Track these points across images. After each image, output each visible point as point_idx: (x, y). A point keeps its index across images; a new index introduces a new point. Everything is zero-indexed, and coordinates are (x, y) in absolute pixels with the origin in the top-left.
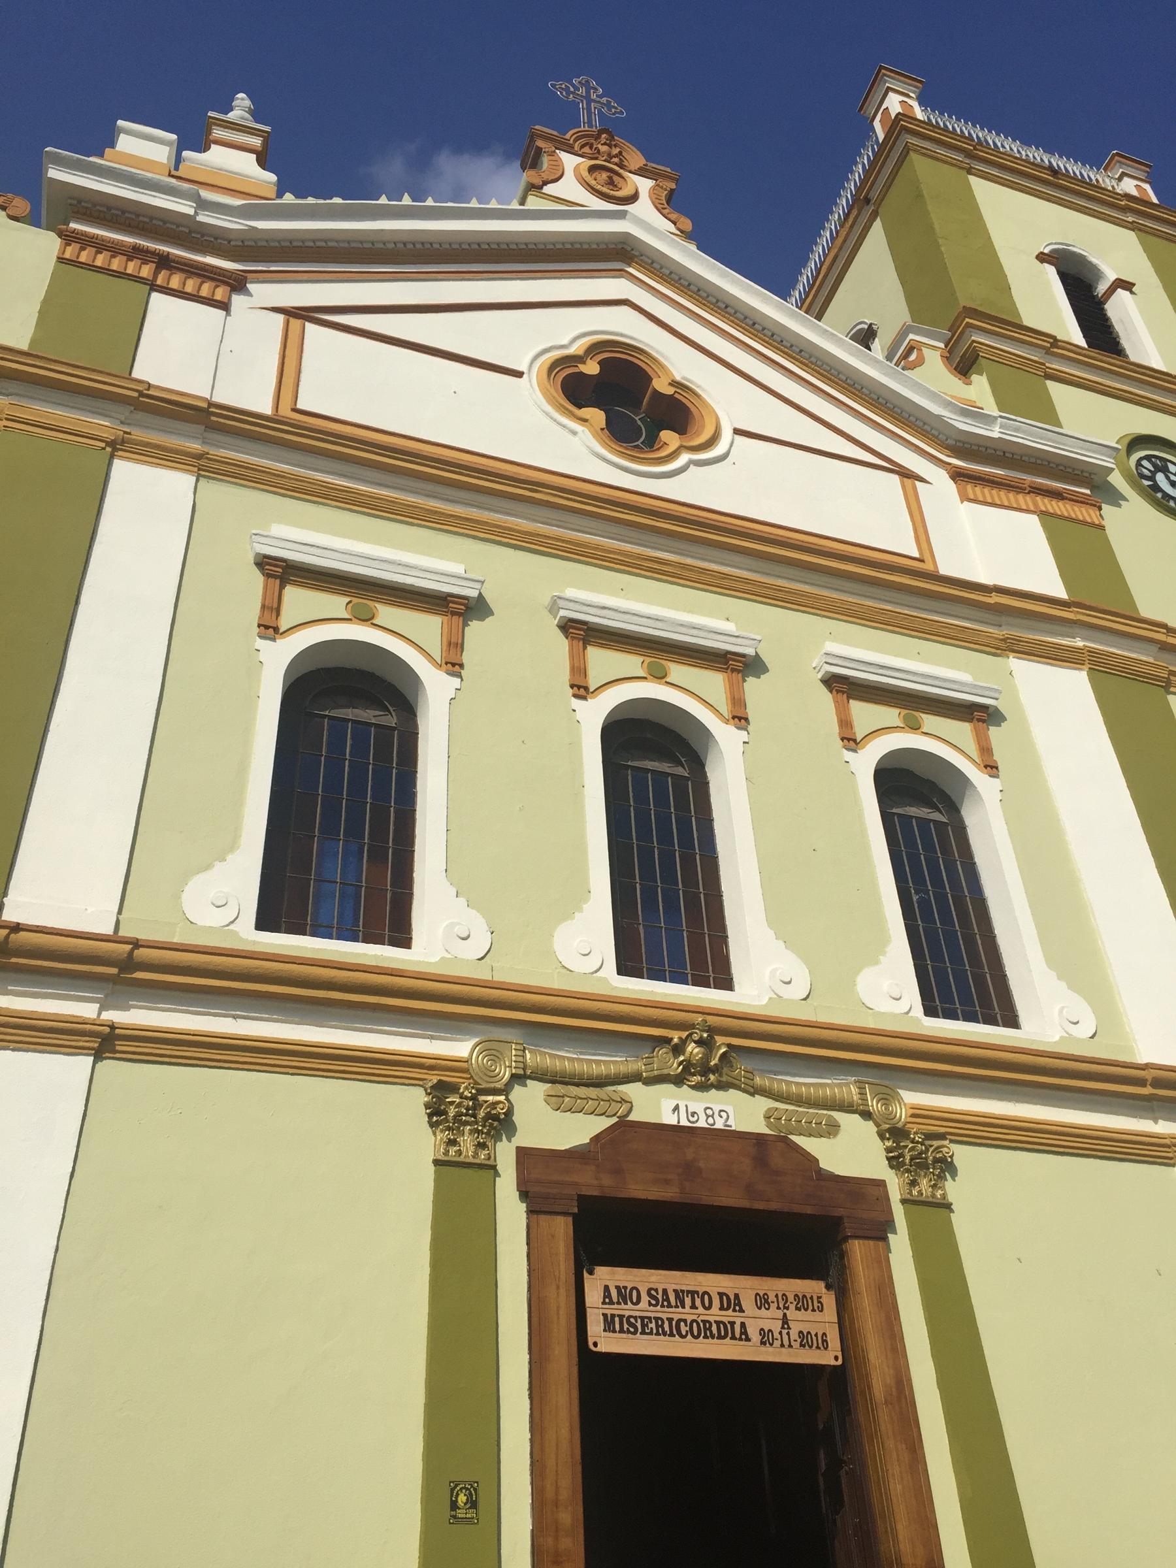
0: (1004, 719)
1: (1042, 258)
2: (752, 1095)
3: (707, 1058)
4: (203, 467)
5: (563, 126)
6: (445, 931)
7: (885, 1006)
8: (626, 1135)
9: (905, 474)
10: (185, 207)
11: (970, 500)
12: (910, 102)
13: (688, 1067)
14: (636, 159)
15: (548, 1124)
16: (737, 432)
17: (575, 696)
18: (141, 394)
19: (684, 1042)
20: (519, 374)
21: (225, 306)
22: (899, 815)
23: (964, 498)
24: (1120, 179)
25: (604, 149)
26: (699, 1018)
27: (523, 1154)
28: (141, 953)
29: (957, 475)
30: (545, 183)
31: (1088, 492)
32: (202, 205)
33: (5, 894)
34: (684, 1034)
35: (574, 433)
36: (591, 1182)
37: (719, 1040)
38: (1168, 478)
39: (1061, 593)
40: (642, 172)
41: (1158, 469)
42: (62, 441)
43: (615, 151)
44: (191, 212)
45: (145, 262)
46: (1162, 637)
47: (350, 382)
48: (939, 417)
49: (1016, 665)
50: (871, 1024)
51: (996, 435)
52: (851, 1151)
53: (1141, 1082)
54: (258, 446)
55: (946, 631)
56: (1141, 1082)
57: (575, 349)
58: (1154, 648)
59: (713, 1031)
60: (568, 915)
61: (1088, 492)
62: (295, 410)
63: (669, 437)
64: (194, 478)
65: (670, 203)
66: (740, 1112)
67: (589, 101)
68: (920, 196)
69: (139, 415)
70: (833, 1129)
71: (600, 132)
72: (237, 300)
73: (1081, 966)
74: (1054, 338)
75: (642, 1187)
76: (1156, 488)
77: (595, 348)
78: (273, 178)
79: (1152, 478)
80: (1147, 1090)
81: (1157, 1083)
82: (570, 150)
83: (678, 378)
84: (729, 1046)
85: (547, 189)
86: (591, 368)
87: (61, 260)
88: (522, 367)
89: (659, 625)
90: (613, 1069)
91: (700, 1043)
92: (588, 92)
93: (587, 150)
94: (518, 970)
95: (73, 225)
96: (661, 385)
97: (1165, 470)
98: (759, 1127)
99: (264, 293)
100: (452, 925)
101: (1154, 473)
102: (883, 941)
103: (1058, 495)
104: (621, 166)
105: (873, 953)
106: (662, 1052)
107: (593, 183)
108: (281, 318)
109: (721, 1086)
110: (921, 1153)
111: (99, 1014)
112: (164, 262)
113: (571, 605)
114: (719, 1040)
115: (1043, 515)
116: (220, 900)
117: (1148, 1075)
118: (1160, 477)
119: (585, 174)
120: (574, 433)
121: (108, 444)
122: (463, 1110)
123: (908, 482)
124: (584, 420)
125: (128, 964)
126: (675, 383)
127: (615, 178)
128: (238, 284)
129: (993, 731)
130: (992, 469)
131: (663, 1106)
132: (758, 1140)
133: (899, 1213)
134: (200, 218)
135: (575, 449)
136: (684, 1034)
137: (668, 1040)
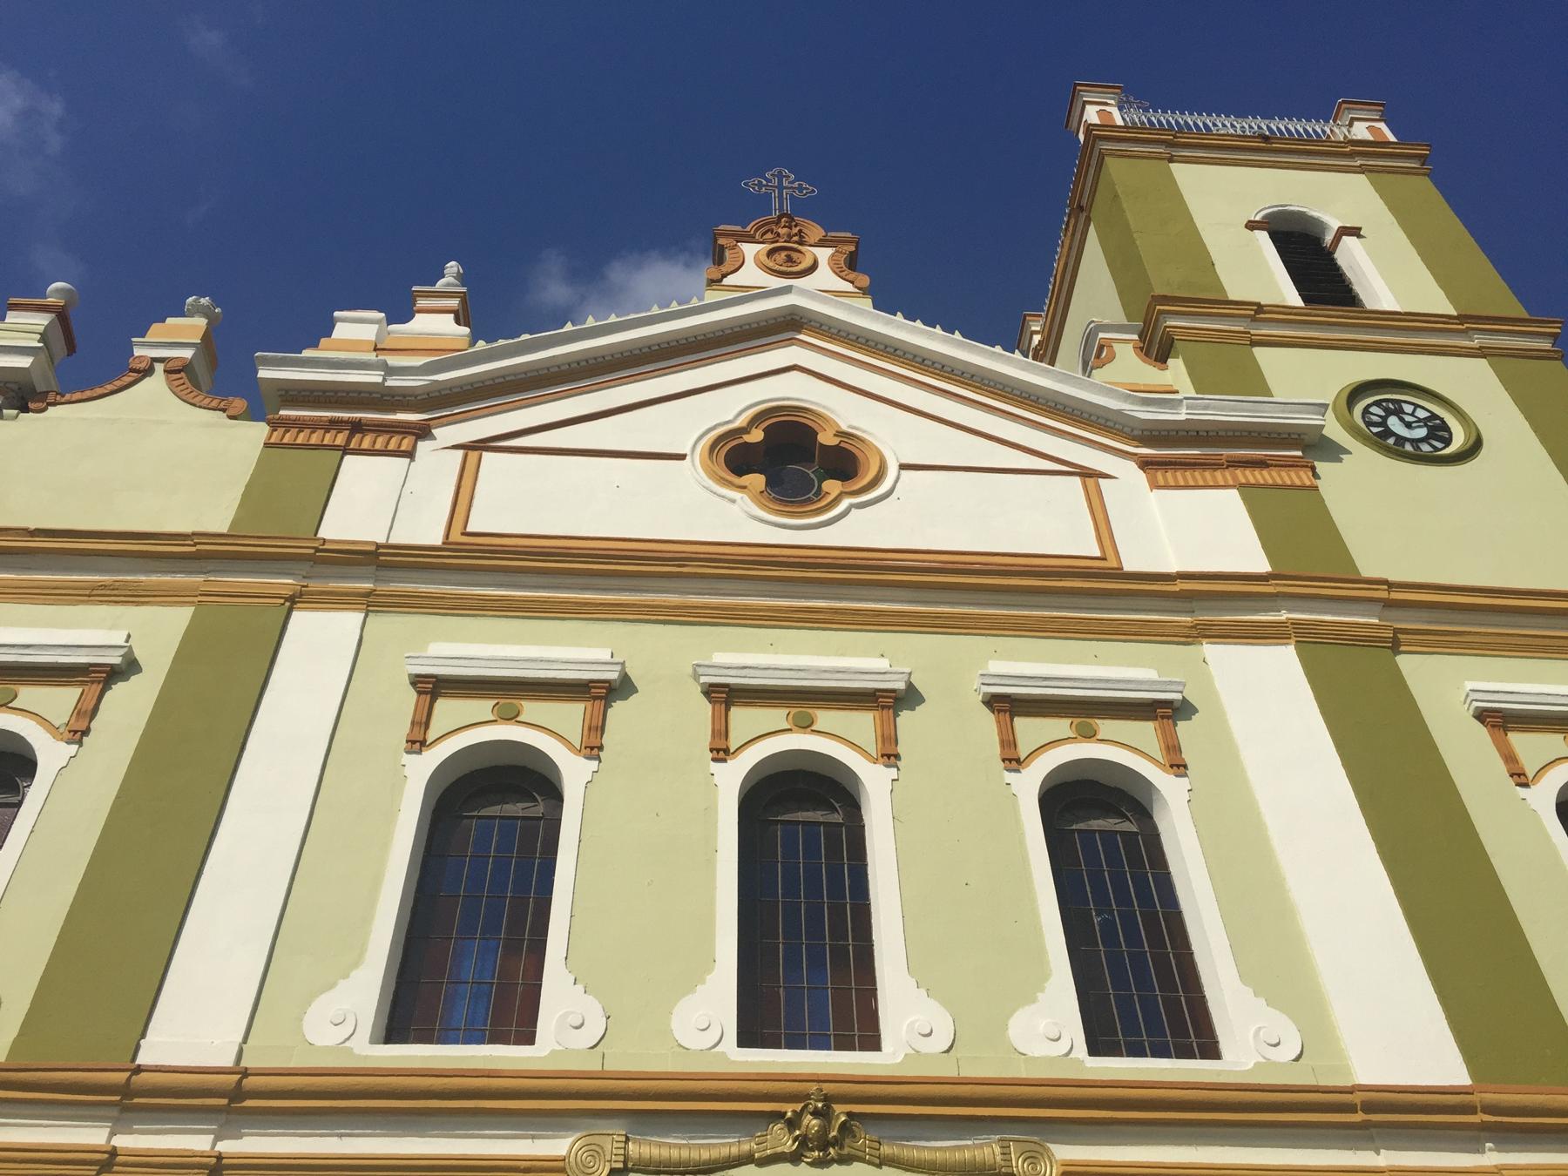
0: (1194, 710)
1: (1252, 226)
2: (879, 1166)
3: (824, 1130)
4: (371, 603)
5: (750, 215)
7: (1040, 1049)
9: (1087, 474)
10: (374, 377)
11: (1159, 487)
12: (1108, 108)
13: (803, 1142)
14: (815, 232)
16: (903, 467)
17: (714, 760)
18: (317, 550)
19: (798, 1115)
20: (682, 457)
21: (410, 454)
22: (1080, 831)
23: (1154, 485)
24: (1351, 125)
25: (783, 231)
26: (814, 1087)
28: (251, 1082)
29: (1146, 464)
30: (724, 276)
31: (1299, 453)
32: (390, 371)
33: (143, 1036)
34: (799, 1107)
35: (734, 501)
37: (838, 1108)
38: (1402, 420)
39: (1262, 565)
40: (822, 243)
41: (1389, 413)
42: (248, 605)
43: (795, 230)
44: (380, 380)
45: (340, 431)
46: (1384, 595)
47: (528, 497)
48: (1119, 412)
49: (1213, 652)
50: (1023, 1073)
51: (1183, 417)
53: (1350, 1108)
54: (414, 575)
55: (1125, 628)
56: (1350, 1108)
57: (741, 422)
58: (1378, 608)
59: (828, 1099)
60: (690, 989)
61: (1299, 453)
62: (465, 534)
63: (832, 487)
64: (362, 615)
65: (851, 264)
67: (780, 187)
68: (1116, 196)
69: (319, 569)
71: (779, 218)
72: (423, 447)
73: (1288, 981)
74: (1258, 304)
76: (1388, 433)
77: (756, 420)
78: (466, 330)
79: (1383, 423)
80: (1359, 1117)
81: (1369, 1107)
82: (751, 239)
83: (845, 428)
84: (850, 1115)
85: (726, 281)
86: (756, 436)
87: (267, 445)
88: (686, 450)
89: (802, 675)
90: (725, 1152)
91: (816, 1113)
92: (780, 182)
93: (769, 236)
95: (282, 412)
96: (826, 438)
97: (1399, 412)
99: (448, 434)
100: (566, 1015)
101: (1385, 419)
102: (1043, 974)
103: (1261, 464)
104: (801, 243)
105: (1027, 993)
106: (778, 1128)
107: (771, 264)
108: (460, 453)
109: (844, 1160)
111: (214, 1145)
112: (357, 427)
113: (711, 671)
114: (838, 1108)
115: (1241, 487)
116: (342, 1020)
117: (1357, 1098)
118: (1394, 423)
119: (764, 258)
120: (734, 501)
121: (287, 600)
123: (1090, 481)
125: (237, 1094)
127: (795, 255)
128: (423, 432)
129: (1182, 726)
130: (1176, 452)
134: (389, 383)
135: (738, 517)
136: (799, 1107)
137: (781, 1115)
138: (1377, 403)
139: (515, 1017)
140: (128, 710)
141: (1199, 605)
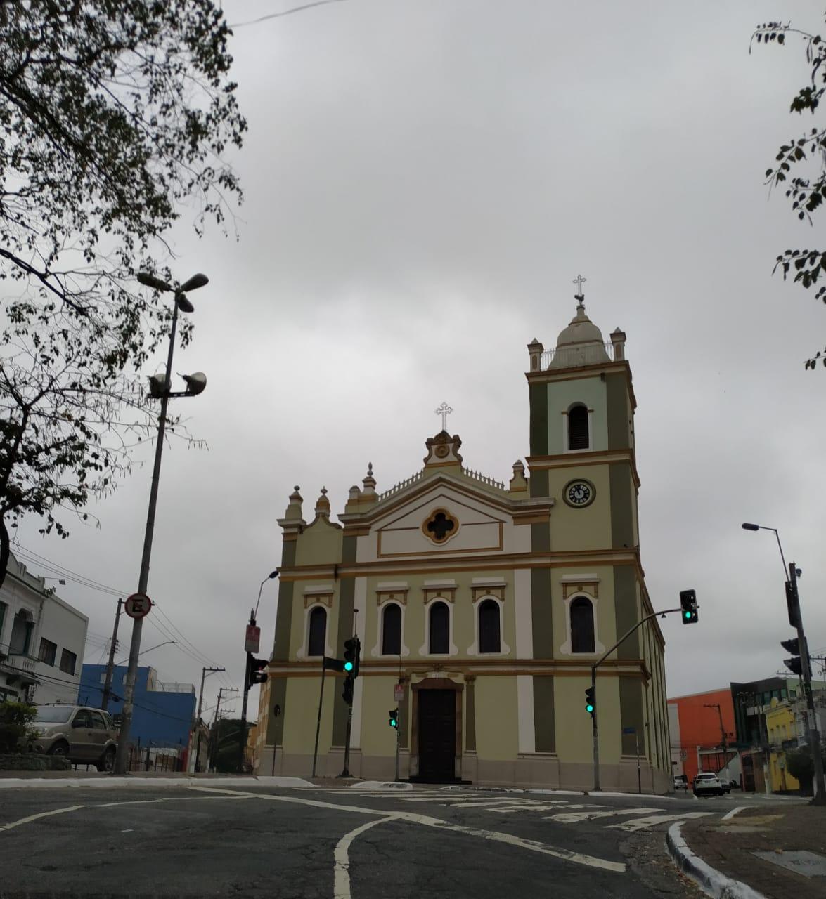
1: (563, 413)
6: (405, 652)
8: (426, 680)
9: (501, 522)
15: (416, 679)
21: (368, 535)
27: (412, 684)
29: (515, 518)
31: (548, 510)
32: (362, 514)
36: (420, 687)
52: (459, 679)
66: (442, 675)
70: (456, 676)
72: (371, 531)
75: (427, 687)
77: (433, 514)
79: (574, 494)
86: (433, 520)
94: (414, 658)
98: (446, 677)
101: (574, 492)
110: (470, 679)
122: (403, 680)
124: (429, 536)
126: (451, 517)
128: (369, 528)
131: (432, 675)
132: (445, 679)
133: (465, 688)
138: (575, 487)
139: (398, 652)
140: (336, 599)
141: (514, 561)
